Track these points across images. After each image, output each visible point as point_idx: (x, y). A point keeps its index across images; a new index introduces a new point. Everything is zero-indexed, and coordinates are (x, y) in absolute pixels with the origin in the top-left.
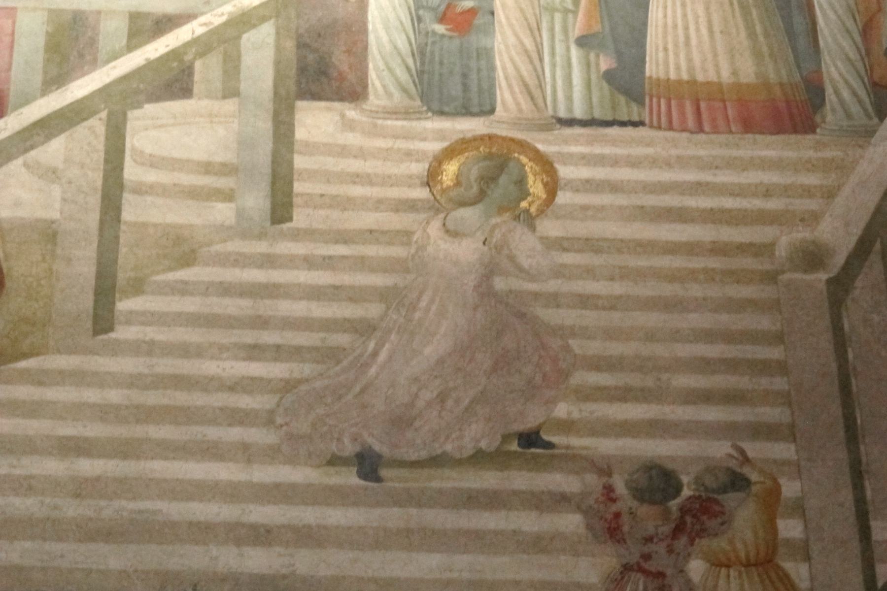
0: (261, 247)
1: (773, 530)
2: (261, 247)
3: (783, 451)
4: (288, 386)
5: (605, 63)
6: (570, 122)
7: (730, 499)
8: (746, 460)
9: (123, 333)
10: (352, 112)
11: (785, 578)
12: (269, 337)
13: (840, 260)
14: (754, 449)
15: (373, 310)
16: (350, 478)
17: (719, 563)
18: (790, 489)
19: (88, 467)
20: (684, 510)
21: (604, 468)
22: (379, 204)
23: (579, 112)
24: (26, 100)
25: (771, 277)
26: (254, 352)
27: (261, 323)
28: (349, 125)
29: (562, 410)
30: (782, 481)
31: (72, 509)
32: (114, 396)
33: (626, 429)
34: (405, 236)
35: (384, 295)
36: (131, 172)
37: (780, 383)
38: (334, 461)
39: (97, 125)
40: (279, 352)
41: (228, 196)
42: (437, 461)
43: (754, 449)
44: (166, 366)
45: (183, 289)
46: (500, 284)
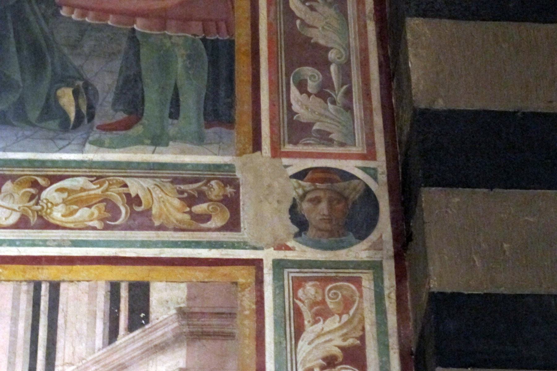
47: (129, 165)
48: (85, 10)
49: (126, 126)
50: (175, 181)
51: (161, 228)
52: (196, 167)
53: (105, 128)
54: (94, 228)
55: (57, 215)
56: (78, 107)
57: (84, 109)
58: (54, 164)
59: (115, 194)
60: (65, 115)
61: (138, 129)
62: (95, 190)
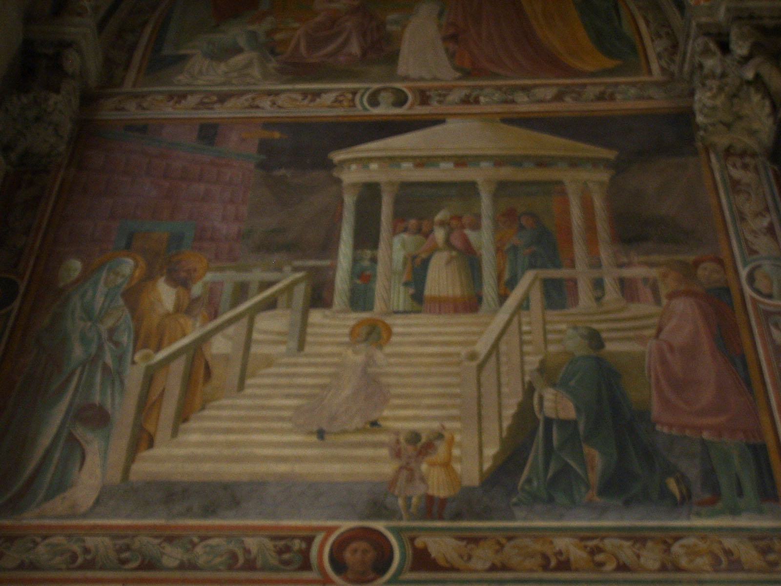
0: (293, 360)
1: (450, 454)
2: (293, 360)
3: (457, 425)
4: (297, 408)
5: (411, 291)
6: (397, 312)
7: (437, 443)
8: (444, 428)
9: (248, 391)
10: (327, 312)
11: (453, 470)
12: (293, 391)
13: (482, 357)
14: (448, 425)
15: (326, 381)
16: (314, 439)
17: (432, 465)
18: (458, 438)
19: (232, 437)
20: (422, 447)
21: (397, 433)
22: (332, 344)
23: (401, 308)
24: (225, 312)
25: (459, 364)
26: (288, 396)
27: (290, 386)
28: (326, 317)
29: (386, 413)
30: (455, 436)
31: (226, 452)
32: (243, 413)
33: (406, 419)
34: (339, 355)
35: (330, 375)
36: (255, 336)
37: (458, 401)
38: (311, 433)
39: (245, 321)
40: (296, 396)
41: (284, 343)
42: (344, 432)
43: (448, 425)
44: (258, 402)
45: (269, 375)
46: (370, 370)
47: (720, 529)
48: (671, 426)
49: (713, 502)
50: (752, 539)
51: (750, 571)
52: (762, 529)
53: (702, 504)
54: (708, 572)
55: (684, 562)
56: (681, 492)
57: (684, 491)
58: (674, 529)
59: (716, 548)
60: (673, 496)
61: (720, 505)
62: (703, 546)
